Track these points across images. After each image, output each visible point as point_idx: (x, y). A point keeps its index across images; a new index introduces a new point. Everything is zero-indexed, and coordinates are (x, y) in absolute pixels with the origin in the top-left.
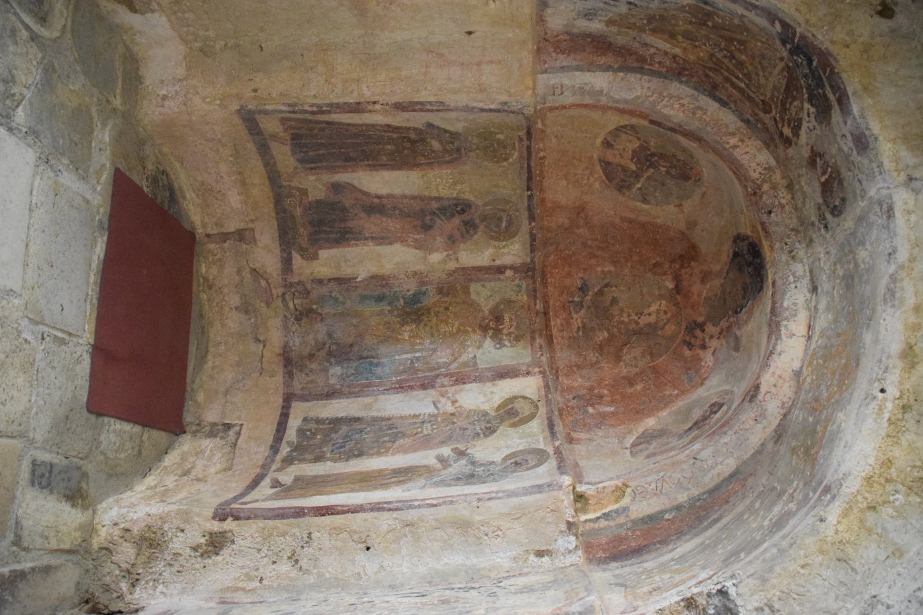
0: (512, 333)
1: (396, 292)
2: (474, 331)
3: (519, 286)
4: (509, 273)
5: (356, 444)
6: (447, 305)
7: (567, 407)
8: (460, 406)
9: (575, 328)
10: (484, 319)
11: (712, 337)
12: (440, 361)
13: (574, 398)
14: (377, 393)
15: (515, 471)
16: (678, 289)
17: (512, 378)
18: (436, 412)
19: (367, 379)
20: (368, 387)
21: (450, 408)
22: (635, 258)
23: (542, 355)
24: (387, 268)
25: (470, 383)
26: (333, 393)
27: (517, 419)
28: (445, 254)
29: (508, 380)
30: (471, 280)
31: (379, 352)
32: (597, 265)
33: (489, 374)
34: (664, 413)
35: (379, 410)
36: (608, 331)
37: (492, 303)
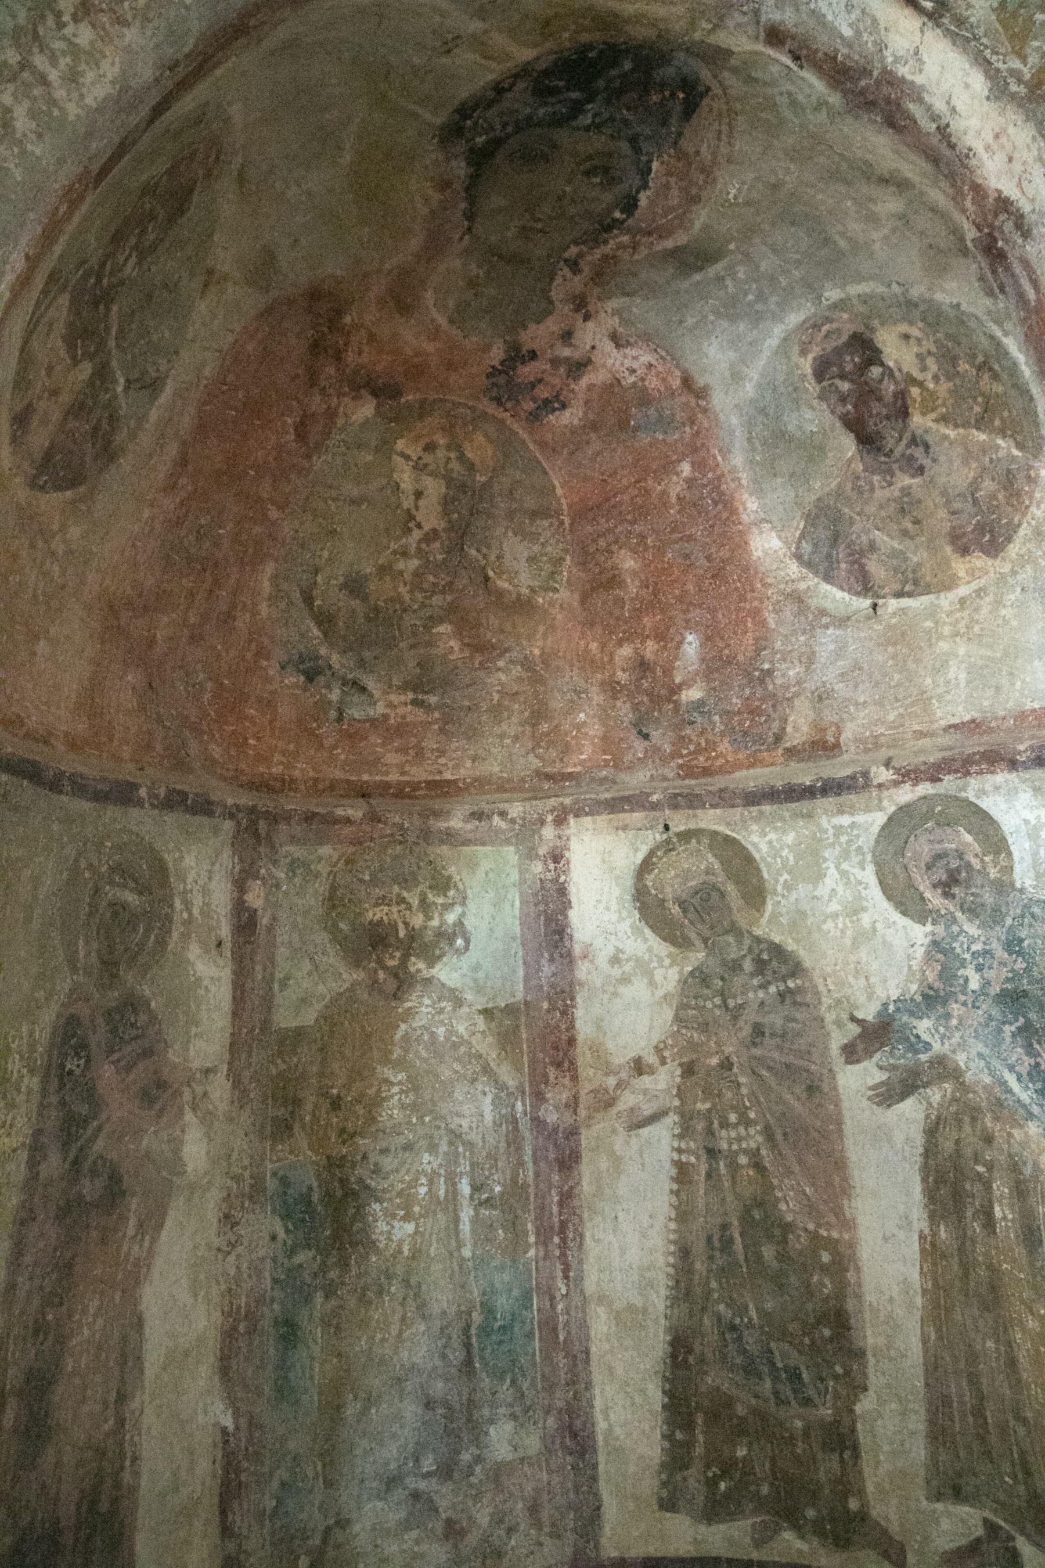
0: (423, 901)
1: (275, 1281)
2: (410, 1014)
3: (294, 865)
4: (255, 897)
5: (784, 1335)
6: (326, 1105)
7: (676, 754)
8: (658, 1050)
9: (420, 715)
10: (374, 985)
11: (567, 336)
12: (489, 1117)
13: (646, 737)
14: (576, 1300)
15: (1004, 886)
16: (384, 391)
17: (567, 905)
18: (673, 1118)
19: (530, 1335)
20: (555, 1330)
21: (664, 1080)
22: (265, 489)
23: (503, 814)
24: (204, 1322)
25: (571, 1026)
26: (575, 1435)
27: (730, 888)
28: (189, 1116)
29: (573, 914)
30: (266, 1025)
31: (454, 1308)
32: (255, 614)
33: (547, 970)
34: (750, 505)
35: (646, 1285)
36: (433, 620)
37: (333, 959)
